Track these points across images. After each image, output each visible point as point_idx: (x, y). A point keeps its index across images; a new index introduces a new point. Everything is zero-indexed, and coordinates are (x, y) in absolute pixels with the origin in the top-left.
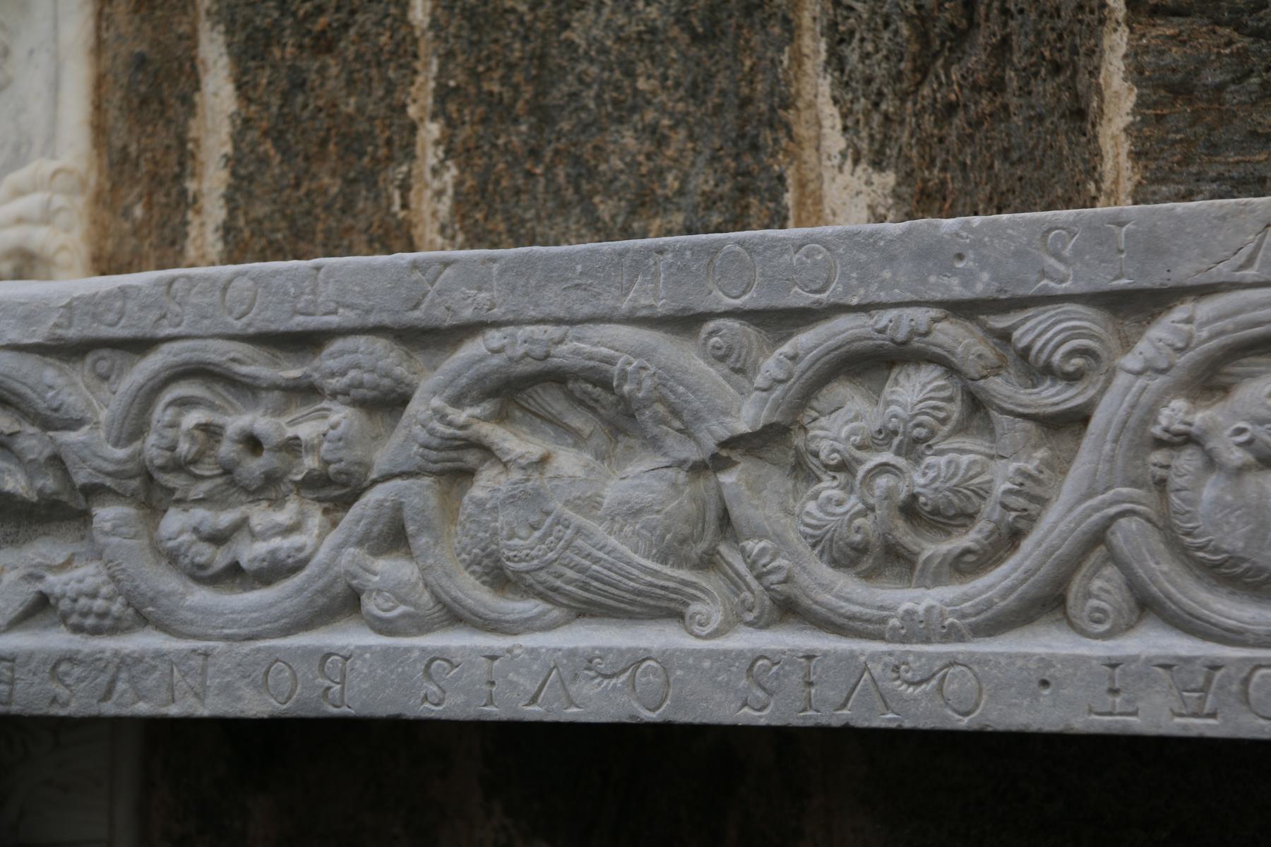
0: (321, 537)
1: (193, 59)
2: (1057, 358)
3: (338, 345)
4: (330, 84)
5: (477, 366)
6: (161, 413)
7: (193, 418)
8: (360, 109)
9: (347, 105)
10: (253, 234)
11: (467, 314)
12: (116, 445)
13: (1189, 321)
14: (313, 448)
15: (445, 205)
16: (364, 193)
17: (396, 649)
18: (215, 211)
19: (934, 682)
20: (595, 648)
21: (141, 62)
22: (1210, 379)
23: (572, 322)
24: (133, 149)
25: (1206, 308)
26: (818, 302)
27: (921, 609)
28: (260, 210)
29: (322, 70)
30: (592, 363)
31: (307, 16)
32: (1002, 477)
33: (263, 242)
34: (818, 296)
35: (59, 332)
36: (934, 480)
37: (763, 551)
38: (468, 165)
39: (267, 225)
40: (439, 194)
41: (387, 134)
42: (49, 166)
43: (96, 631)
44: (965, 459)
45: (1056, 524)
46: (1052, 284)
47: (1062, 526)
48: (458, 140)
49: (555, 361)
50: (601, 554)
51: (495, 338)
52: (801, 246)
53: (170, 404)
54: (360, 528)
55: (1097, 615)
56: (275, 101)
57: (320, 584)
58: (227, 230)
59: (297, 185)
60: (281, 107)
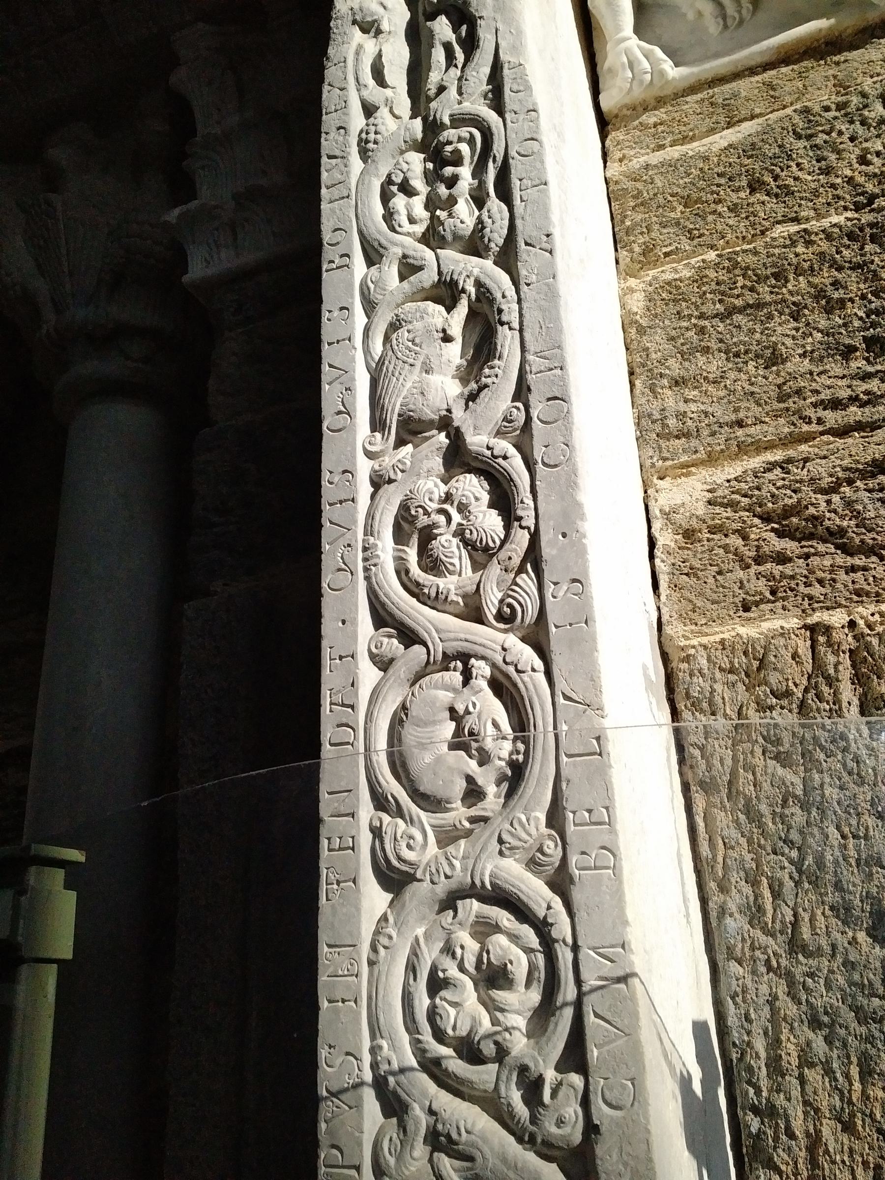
0: (408, 234)
2: (510, 600)
3: (505, 208)
4: (734, 196)
5: (495, 286)
6: (464, 132)
7: (464, 148)
10: (645, 181)
11: (523, 272)
12: (451, 115)
13: (533, 670)
14: (450, 215)
15: (668, 276)
16: (672, 231)
17: (353, 290)
18: (656, 158)
19: (344, 566)
20: (355, 390)
22: (503, 688)
23: (521, 331)
25: (541, 678)
26: (536, 463)
27: (379, 553)
30: (499, 348)
32: (448, 584)
34: (540, 461)
35: (506, 66)
36: (443, 546)
37: (404, 464)
38: (693, 281)
40: (676, 271)
43: (360, 140)
44: (456, 561)
45: (423, 615)
46: (551, 590)
47: (421, 618)
48: (707, 272)
49: (499, 328)
50: (401, 380)
51: (511, 292)
52: (567, 445)
53: (471, 133)
54: (411, 253)
55: (379, 645)
56: (721, 169)
57: (384, 242)
58: (647, 167)
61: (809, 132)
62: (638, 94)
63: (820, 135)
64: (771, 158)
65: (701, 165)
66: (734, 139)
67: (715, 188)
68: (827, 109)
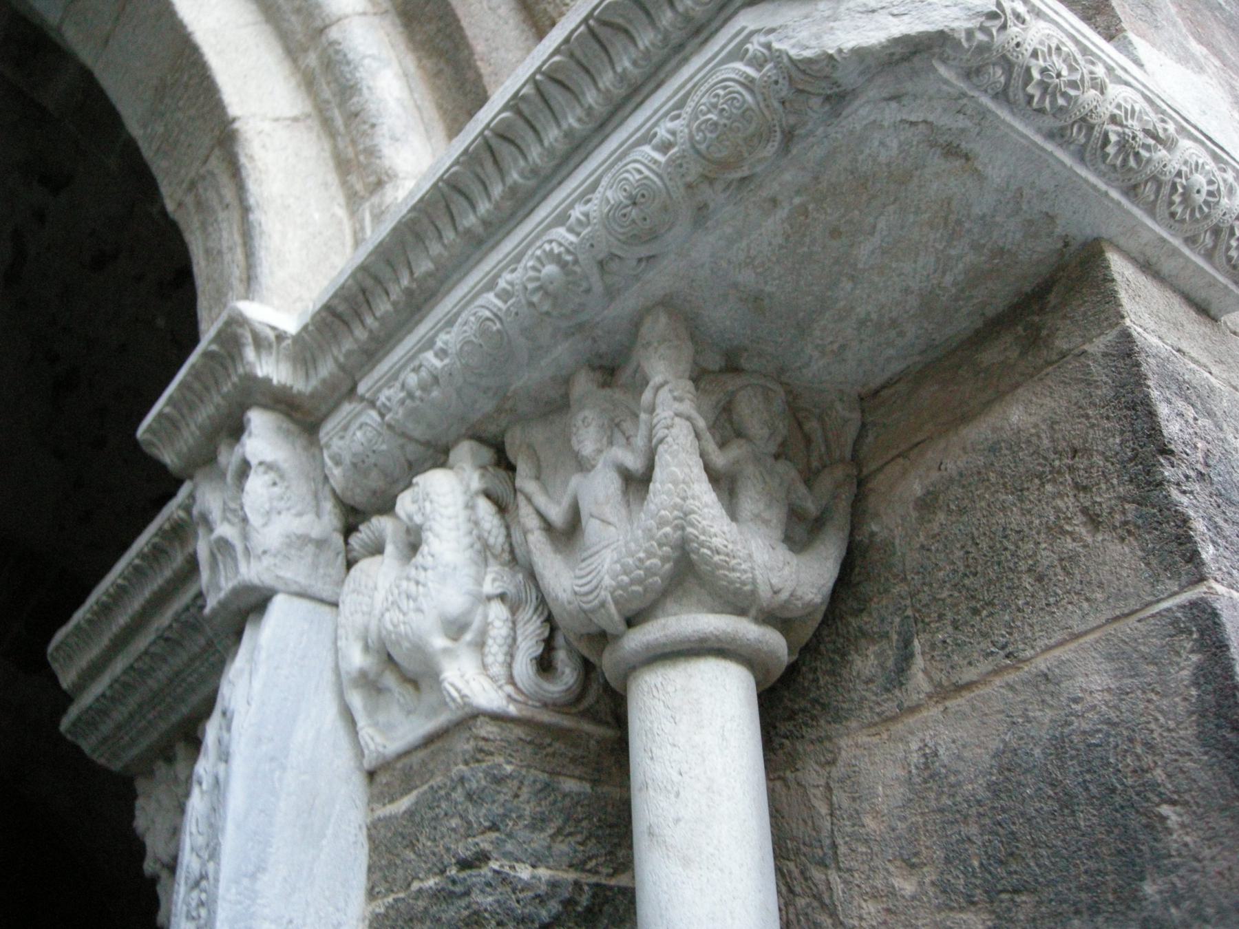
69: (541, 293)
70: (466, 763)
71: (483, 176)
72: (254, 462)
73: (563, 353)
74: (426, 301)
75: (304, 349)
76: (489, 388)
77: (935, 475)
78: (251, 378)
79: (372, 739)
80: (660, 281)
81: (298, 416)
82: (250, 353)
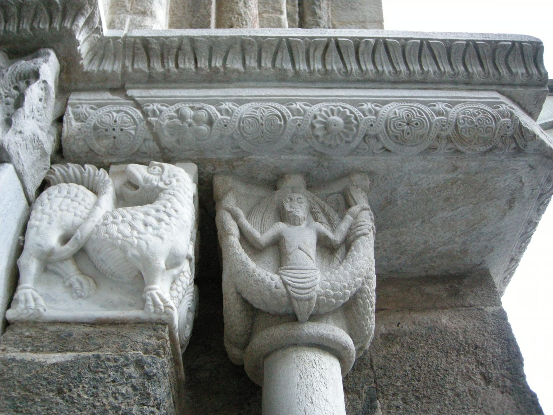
1: (67, 351)
4: (47, 393)
8: (35, 403)
9: (38, 398)
10: (9, 367)
18: (19, 356)
21: (70, 335)
24: (46, 332)
28: (15, 371)
29: (52, 391)
31: (70, 386)
33: (5, 371)
39: (10, 372)
41: (24, 412)
42: (41, 309)
56: (46, 376)
58: (13, 360)
59: (19, 382)
60: (44, 377)
61: (96, 370)
62: (24, 317)
63: (100, 374)
64: (72, 378)
65: (38, 369)
66: (59, 360)
67: (39, 385)
68: (109, 360)
69: (322, 125)
70: (146, 352)
71: (311, 54)
72: (42, 77)
73: (300, 159)
74: (219, 81)
75: (103, 48)
76: (239, 147)
77: (395, 327)
78: (71, 35)
79: (35, 300)
80: (380, 163)
81: (64, 77)
82: (81, 21)
